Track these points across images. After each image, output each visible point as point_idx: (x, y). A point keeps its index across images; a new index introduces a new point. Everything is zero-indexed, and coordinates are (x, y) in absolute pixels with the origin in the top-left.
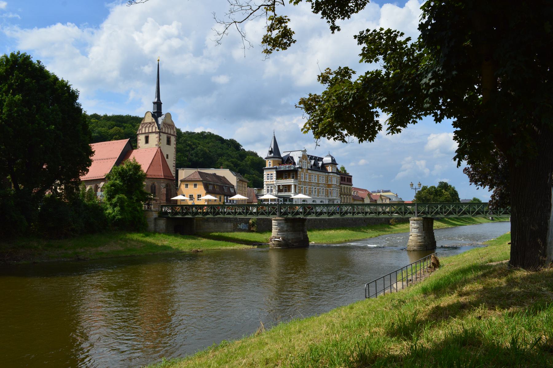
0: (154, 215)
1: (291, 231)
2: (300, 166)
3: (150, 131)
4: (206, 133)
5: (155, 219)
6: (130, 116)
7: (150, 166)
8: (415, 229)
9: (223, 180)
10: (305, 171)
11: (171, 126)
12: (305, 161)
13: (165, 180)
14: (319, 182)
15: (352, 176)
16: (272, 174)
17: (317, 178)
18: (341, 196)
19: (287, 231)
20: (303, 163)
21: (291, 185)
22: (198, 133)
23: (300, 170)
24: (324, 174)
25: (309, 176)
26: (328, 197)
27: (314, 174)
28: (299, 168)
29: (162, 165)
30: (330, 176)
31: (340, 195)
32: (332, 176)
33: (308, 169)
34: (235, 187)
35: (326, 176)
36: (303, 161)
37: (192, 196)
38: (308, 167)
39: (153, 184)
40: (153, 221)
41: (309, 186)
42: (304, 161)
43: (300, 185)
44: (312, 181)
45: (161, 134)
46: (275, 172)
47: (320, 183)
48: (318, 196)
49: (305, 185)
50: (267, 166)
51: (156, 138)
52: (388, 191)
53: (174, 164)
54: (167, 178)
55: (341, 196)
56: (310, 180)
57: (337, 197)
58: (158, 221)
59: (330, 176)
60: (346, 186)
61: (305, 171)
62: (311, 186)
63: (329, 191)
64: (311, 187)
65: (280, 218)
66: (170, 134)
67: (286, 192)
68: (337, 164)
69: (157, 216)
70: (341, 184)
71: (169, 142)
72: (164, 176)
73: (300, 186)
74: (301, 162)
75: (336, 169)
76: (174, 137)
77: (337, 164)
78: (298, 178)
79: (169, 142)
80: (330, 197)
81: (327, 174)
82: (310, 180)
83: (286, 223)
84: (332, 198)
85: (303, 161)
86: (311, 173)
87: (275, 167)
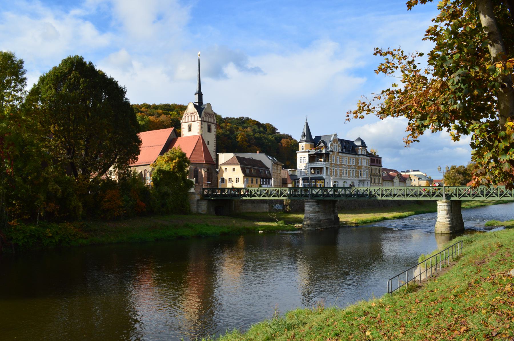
0: (197, 197)
1: (322, 213)
2: (332, 149)
3: (193, 120)
4: (244, 118)
5: (198, 201)
6: (176, 104)
7: (193, 152)
8: (443, 211)
9: (259, 164)
10: (336, 154)
12: (336, 145)
13: (206, 165)
14: (350, 164)
15: (381, 158)
16: (305, 158)
17: (347, 160)
18: (371, 177)
19: (318, 212)
21: (323, 167)
22: (237, 119)
23: (331, 153)
24: (354, 156)
25: (340, 159)
26: (358, 178)
27: (345, 157)
28: (330, 151)
29: (204, 151)
30: (360, 158)
31: (370, 176)
32: (362, 158)
33: (339, 152)
34: (270, 170)
35: (357, 158)
36: (334, 144)
37: (231, 179)
38: (338, 150)
39: (196, 168)
40: (196, 203)
42: (335, 144)
43: (331, 166)
44: (343, 164)
45: (203, 122)
46: (308, 156)
47: (350, 165)
48: (349, 177)
49: (336, 167)
50: (300, 150)
51: (199, 126)
52: (418, 171)
53: (214, 149)
54: (208, 163)
56: (341, 163)
57: (367, 178)
58: (200, 203)
59: (360, 158)
60: (376, 167)
61: (336, 154)
62: (342, 168)
63: (359, 172)
64: (342, 169)
65: (312, 201)
66: (211, 123)
67: (319, 174)
68: (367, 147)
69: (199, 199)
71: (209, 130)
72: (205, 161)
73: (332, 168)
74: (333, 145)
75: (366, 151)
77: (367, 147)
78: (329, 160)
79: (209, 130)
80: (360, 178)
81: (357, 156)
82: (341, 163)
83: (317, 205)
84: (363, 179)
85: (334, 144)
86: (342, 156)
87: (307, 150)
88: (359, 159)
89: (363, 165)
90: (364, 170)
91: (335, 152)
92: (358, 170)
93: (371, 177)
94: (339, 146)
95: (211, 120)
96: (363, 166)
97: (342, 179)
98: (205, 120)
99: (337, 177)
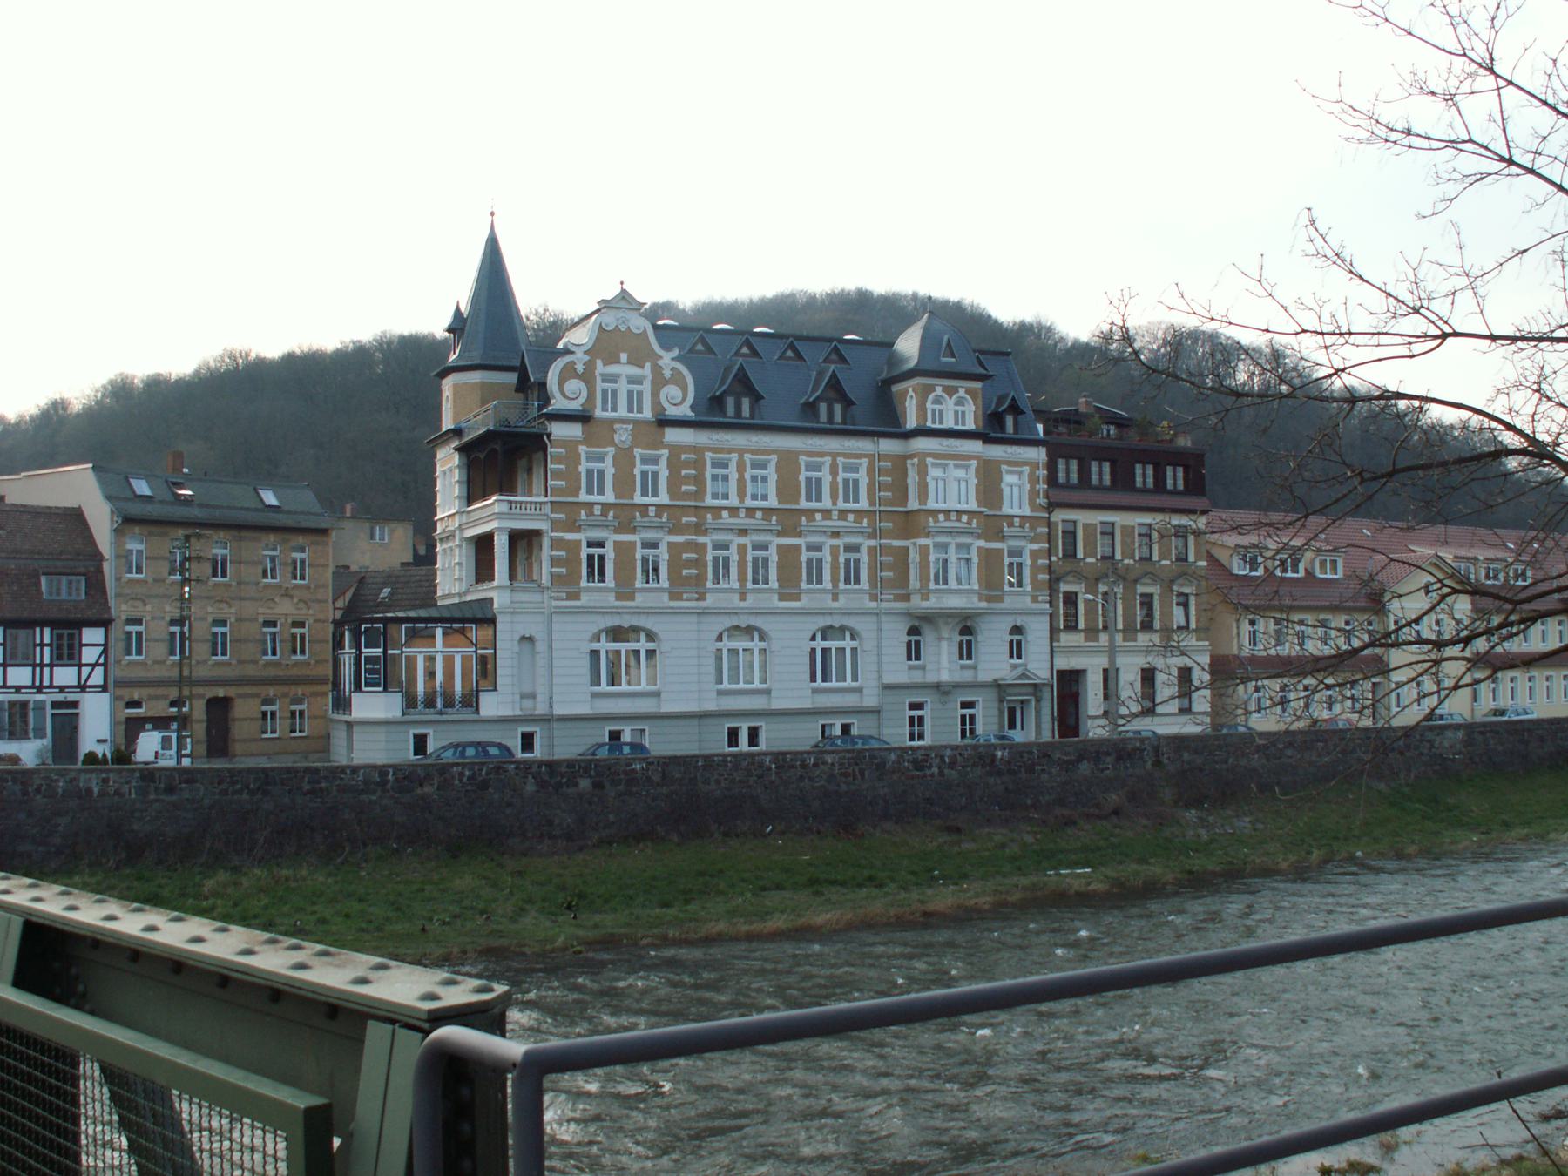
2: (575, 405)
12: (633, 371)
20: (600, 385)
25: (674, 465)
26: (907, 598)
30: (911, 456)
33: (663, 422)
35: (881, 457)
42: (613, 369)
43: (573, 526)
44: (709, 501)
47: (810, 513)
49: (626, 526)
59: (911, 456)
61: (623, 436)
70: (1052, 506)
74: (587, 377)
80: (918, 604)
81: (888, 446)
82: (700, 493)
85: (600, 368)
86: (698, 450)
88: (909, 461)
89: (931, 504)
90: (953, 541)
92: (896, 543)
94: (659, 382)
96: (934, 513)
97: (702, 613)
99: (640, 600)
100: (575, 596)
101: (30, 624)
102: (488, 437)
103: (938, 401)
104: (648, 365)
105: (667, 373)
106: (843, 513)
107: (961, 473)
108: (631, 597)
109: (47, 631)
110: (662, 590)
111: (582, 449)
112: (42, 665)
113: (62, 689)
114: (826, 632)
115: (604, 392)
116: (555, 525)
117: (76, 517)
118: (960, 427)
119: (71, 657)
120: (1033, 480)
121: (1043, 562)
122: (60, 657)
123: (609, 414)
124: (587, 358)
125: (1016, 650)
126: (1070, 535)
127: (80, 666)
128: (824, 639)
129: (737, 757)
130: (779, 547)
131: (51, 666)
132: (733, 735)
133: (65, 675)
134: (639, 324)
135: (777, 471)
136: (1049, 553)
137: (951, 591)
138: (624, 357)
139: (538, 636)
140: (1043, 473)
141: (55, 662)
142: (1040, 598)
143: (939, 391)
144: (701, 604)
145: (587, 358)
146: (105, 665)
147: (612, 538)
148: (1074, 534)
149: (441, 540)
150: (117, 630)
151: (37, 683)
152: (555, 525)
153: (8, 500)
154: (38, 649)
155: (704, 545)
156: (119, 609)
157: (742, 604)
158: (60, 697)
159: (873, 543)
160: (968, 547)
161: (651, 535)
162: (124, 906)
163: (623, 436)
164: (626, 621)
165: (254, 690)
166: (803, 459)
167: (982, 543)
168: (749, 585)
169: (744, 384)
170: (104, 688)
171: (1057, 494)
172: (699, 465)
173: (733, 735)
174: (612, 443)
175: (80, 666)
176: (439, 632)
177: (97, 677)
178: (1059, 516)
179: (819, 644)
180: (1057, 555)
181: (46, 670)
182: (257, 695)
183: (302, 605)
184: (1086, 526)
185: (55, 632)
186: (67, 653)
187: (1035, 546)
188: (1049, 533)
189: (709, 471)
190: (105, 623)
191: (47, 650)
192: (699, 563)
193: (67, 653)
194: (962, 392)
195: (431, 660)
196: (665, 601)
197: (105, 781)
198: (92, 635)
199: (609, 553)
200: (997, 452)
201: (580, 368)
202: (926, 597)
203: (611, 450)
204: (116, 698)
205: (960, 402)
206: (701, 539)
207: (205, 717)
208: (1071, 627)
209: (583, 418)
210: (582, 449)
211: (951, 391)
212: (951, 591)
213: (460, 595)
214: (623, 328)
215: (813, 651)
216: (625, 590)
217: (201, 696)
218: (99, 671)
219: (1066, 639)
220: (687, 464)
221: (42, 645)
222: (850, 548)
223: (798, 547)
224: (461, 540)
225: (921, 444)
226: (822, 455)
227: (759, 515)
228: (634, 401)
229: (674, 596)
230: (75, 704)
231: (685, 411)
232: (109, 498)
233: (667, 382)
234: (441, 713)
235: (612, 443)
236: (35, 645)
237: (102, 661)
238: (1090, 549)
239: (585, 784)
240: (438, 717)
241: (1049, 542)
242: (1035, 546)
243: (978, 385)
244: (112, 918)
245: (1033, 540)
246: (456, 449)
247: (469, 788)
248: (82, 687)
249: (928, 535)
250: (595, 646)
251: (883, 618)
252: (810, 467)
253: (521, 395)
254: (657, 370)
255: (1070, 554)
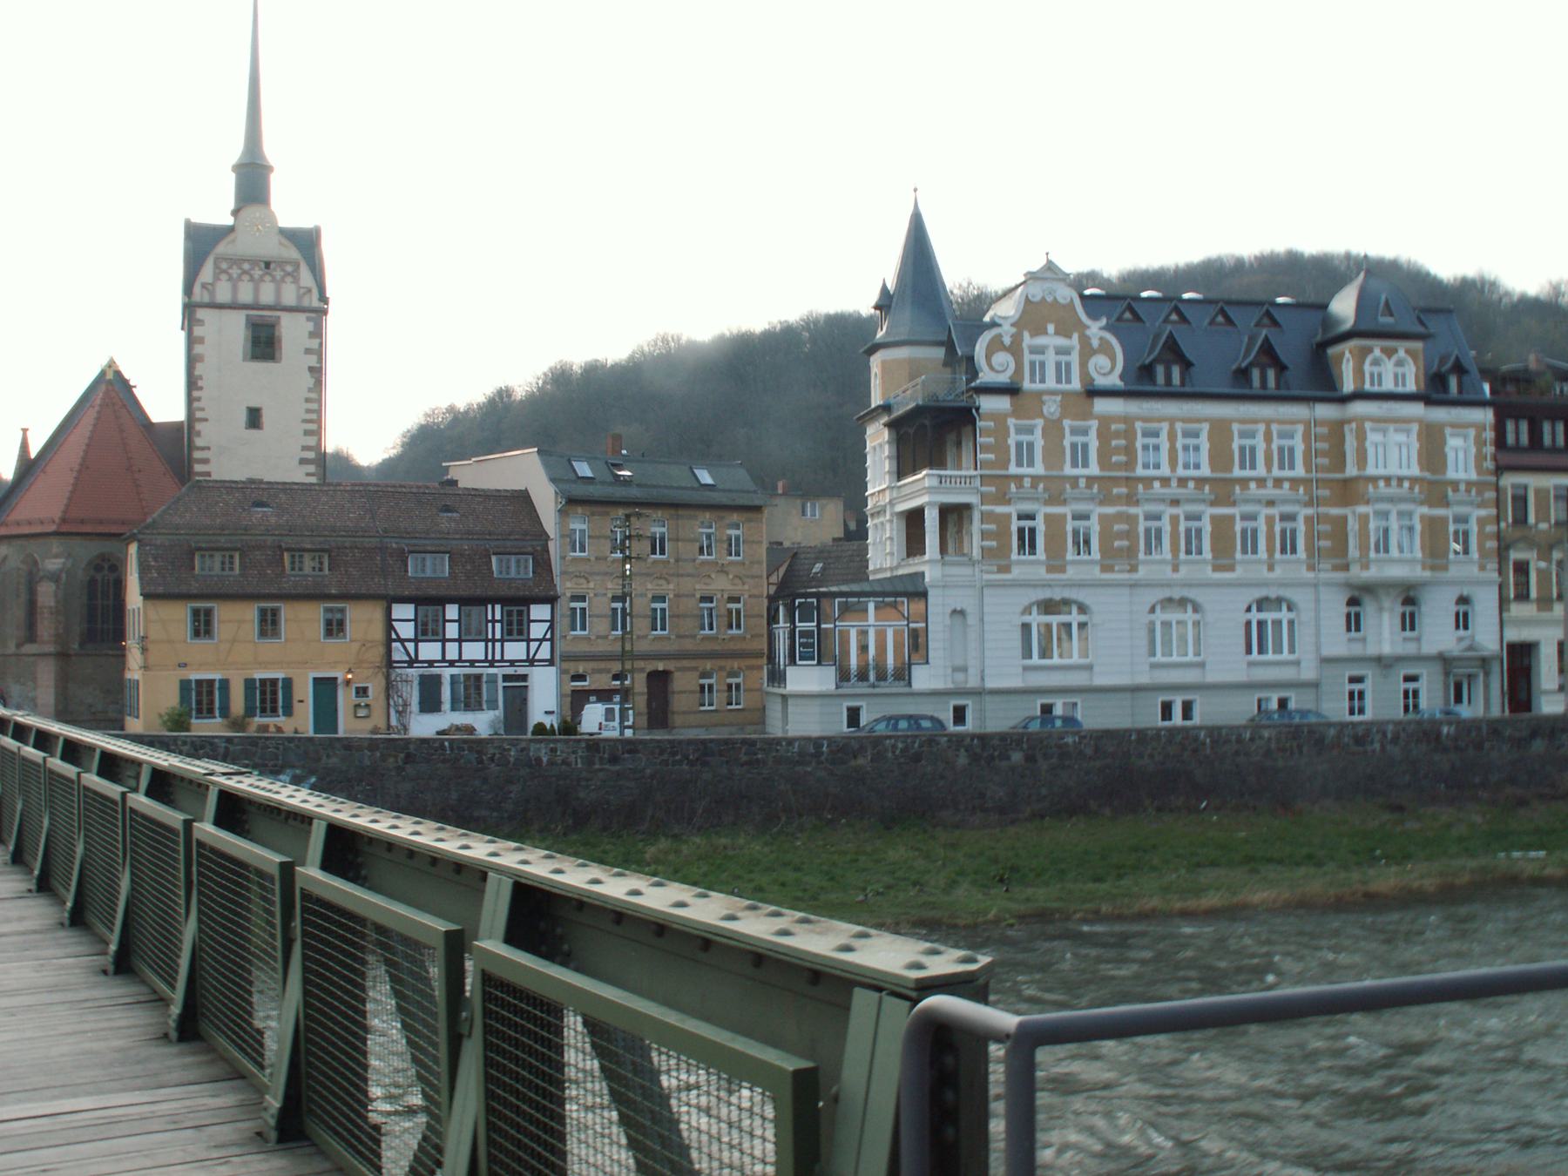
2: (1003, 378)
11: (282, 263)
12: (1061, 341)
25: (1104, 435)
26: (1346, 568)
30: (1349, 421)
33: (1092, 392)
35: (1323, 423)
41: (1106, 500)
42: (1040, 341)
43: (1003, 498)
45: (201, 314)
47: (1244, 482)
49: (1056, 499)
53: (305, 448)
54: (88, 529)
55: (1515, 555)
59: (1349, 421)
61: (1052, 407)
70: (1500, 470)
73: (1000, 509)
74: (1015, 349)
76: (302, 317)
80: (1358, 574)
81: (1325, 411)
82: (1130, 464)
86: (1128, 420)
89: (1371, 470)
90: (1394, 510)
91: (1039, 395)
92: (1335, 511)
93: (1515, 555)
94: (1087, 352)
95: (278, 292)
96: (1374, 480)
97: (1133, 585)
98: (223, 293)
100: (1005, 569)
101: (483, 601)
102: (917, 412)
103: (1376, 362)
104: (1076, 336)
105: (1095, 343)
106: (1278, 482)
107: (1402, 438)
108: (1062, 569)
109: (498, 608)
110: (1092, 562)
111: (1011, 422)
112: (494, 641)
113: (512, 663)
114: (1262, 604)
115: (1032, 364)
116: (985, 498)
117: (522, 499)
118: (1400, 389)
119: (520, 632)
120: (1480, 443)
121: (1491, 528)
122: (510, 633)
123: (1038, 386)
124: (1014, 330)
125: (1462, 621)
126: (1521, 501)
127: (529, 641)
128: (1259, 610)
129: (1173, 731)
130: (1213, 518)
131: (502, 641)
132: (1167, 710)
133: (515, 650)
134: (1065, 294)
135: (1210, 438)
136: (1498, 519)
137: (1393, 561)
138: (1051, 328)
139: (969, 610)
140: (1490, 435)
141: (506, 637)
142: (1488, 567)
143: (1377, 352)
144: (1135, 576)
145: (1014, 330)
146: (552, 640)
147: (1042, 511)
148: (1525, 499)
149: (872, 515)
150: (564, 605)
151: (490, 658)
152: (985, 498)
153: (460, 485)
154: (490, 625)
155: (1136, 516)
156: (564, 586)
157: (1175, 576)
158: (510, 671)
159: (1310, 511)
160: (1410, 515)
161: (1082, 507)
162: (606, 870)
163: (1052, 407)
164: (1057, 594)
165: (693, 663)
166: (1236, 427)
167: (1425, 510)
168: (1182, 556)
169: (1173, 352)
170: (551, 662)
171: (1506, 457)
172: (1129, 435)
173: (1167, 710)
174: (1041, 415)
175: (529, 641)
176: (871, 606)
177: (545, 652)
178: (1509, 480)
179: (1255, 616)
180: (1506, 520)
181: (498, 645)
182: (695, 669)
183: (737, 581)
184: (1537, 492)
185: (505, 608)
186: (517, 629)
187: (1483, 512)
188: (1498, 499)
189: (1140, 442)
190: (551, 600)
191: (498, 625)
192: (1130, 534)
193: (517, 629)
194: (1402, 353)
195: (863, 633)
196: (1096, 573)
197: (553, 750)
198: (540, 612)
199: (1040, 525)
200: (1440, 414)
201: (1007, 340)
202: (1366, 566)
203: (1040, 422)
204: (562, 672)
205: (1400, 363)
206: (1133, 510)
207: (646, 690)
208: (1523, 596)
209: (1012, 390)
210: (1011, 422)
211: (1390, 353)
212: (1393, 561)
213: (891, 569)
214: (1050, 299)
215: (1248, 624)
216: (1056, 563)
217: (642, 670)
218: (546, 645)
219: (1517, 610)
220: (1117, 435)
221: (494, 621)
222: (1285, 517)
223: (1231, 518)
224: (892, 515)
225: (1359, 408)
226: (1255, 421)
227: (1191, 484)
228: (1062, 372)
229: (1106, 568)
230: (524, 678)
231: (1114, 380)
232: (553, 480)
233: (1094, 352)
234: (873, 686)
235: (1041, 415)
236: (488, 621)
237: (548, 636)
238: (1543, 514)
239: (1017, 757)
240: (870, 690)
241: (1498, 507)
242: (1483, 512)
243: (1418, 345)
244: (596, 882)
245: (1482, 505)
246: (885, 425)
247: (902, 760)
248: (531, 662)
249: (1368, 502)
250: (1027, 619)
251: (1321, 589)
252: (1243, 435)
253: (949, 370)
254: (1085, 341)
255: (1520, 519)
